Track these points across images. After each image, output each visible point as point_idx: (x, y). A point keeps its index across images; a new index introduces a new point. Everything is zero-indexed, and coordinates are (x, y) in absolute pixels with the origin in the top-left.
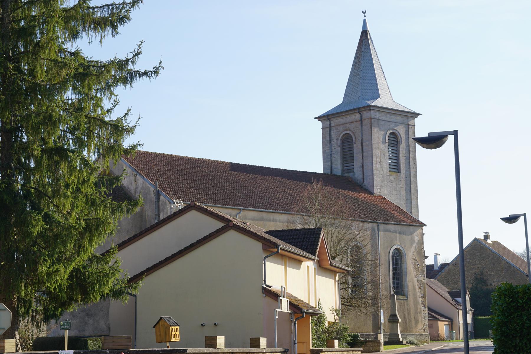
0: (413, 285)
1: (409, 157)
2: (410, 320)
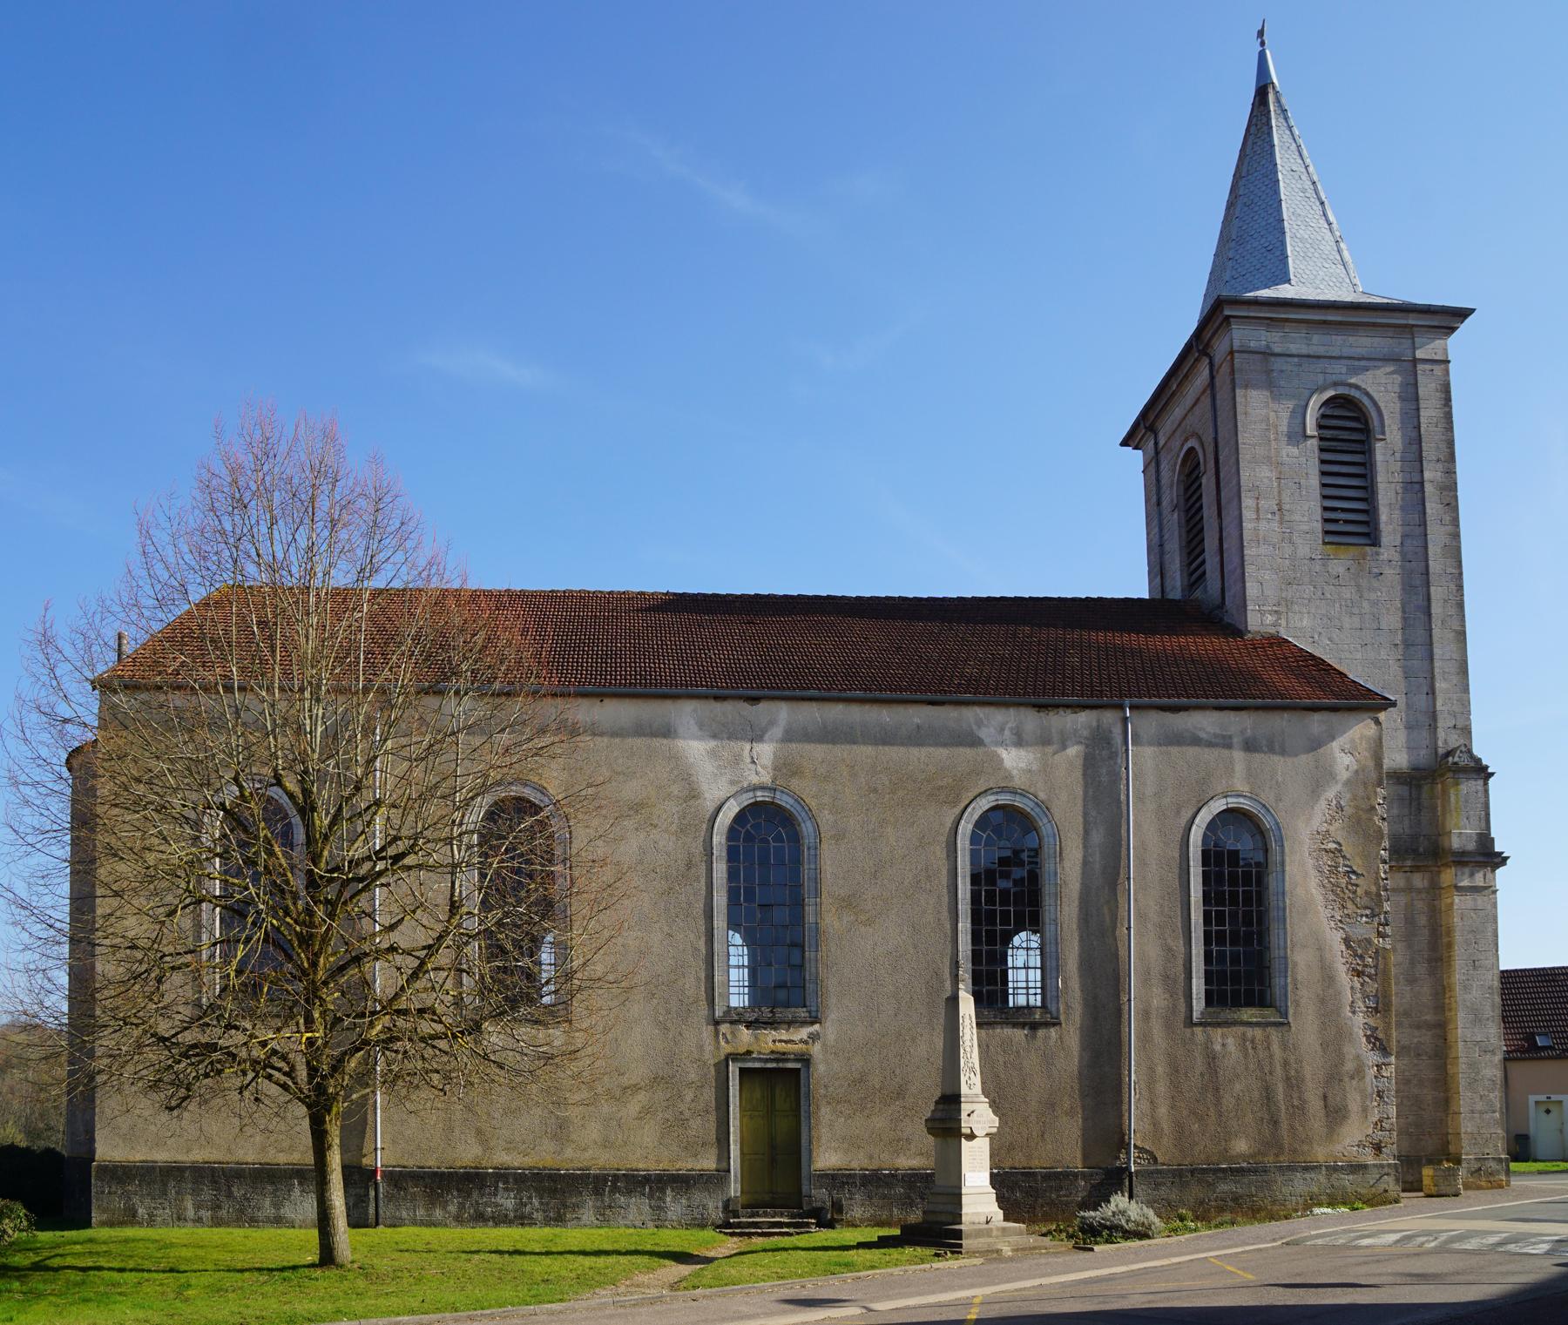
0: (1322, 959)
1: (1422, 483)
2: (1299, 1110)
